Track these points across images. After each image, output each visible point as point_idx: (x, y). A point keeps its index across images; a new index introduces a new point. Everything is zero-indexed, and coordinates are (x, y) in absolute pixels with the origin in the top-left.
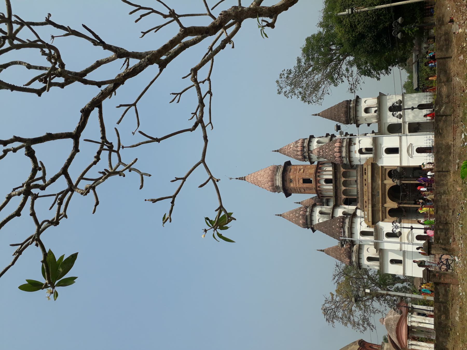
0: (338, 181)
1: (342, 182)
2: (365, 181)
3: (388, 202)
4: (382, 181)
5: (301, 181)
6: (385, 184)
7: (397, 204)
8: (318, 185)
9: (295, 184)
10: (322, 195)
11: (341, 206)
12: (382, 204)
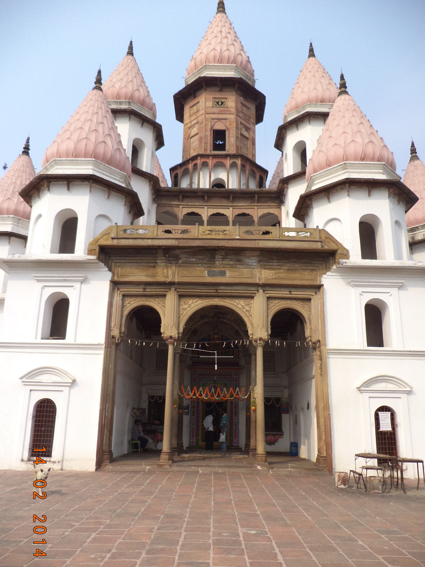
0: (225, 203)
1: (222, 211)
2: (264, 233)
3: (186, 306)
4: (265, 286)
5: (219, 126)
6: (253, 297)
7: (177, 336)
8: (211, 162)
9: (209, 110)
10: (180, 175)
11: (155, 206)
12: (179, 284)
